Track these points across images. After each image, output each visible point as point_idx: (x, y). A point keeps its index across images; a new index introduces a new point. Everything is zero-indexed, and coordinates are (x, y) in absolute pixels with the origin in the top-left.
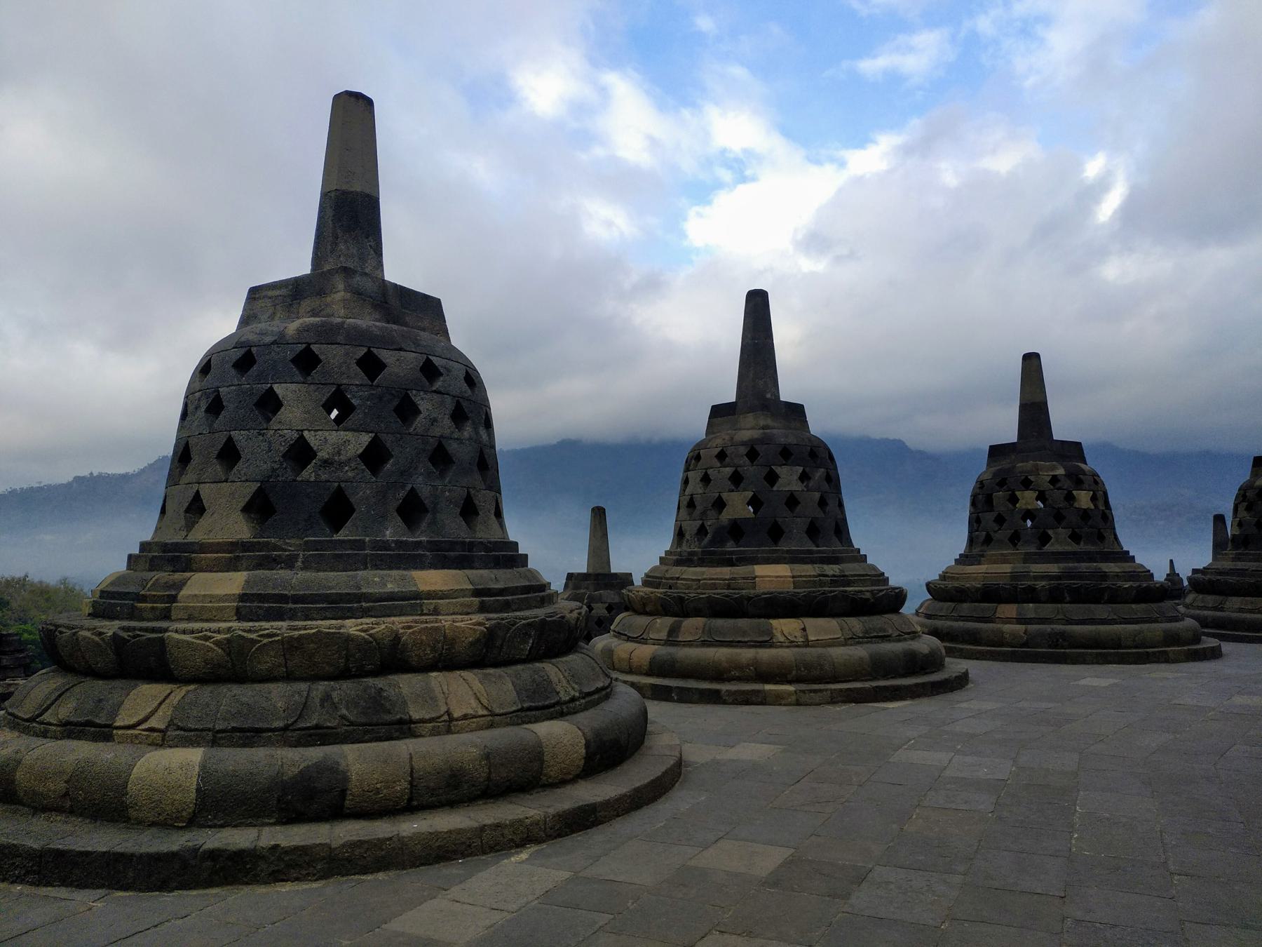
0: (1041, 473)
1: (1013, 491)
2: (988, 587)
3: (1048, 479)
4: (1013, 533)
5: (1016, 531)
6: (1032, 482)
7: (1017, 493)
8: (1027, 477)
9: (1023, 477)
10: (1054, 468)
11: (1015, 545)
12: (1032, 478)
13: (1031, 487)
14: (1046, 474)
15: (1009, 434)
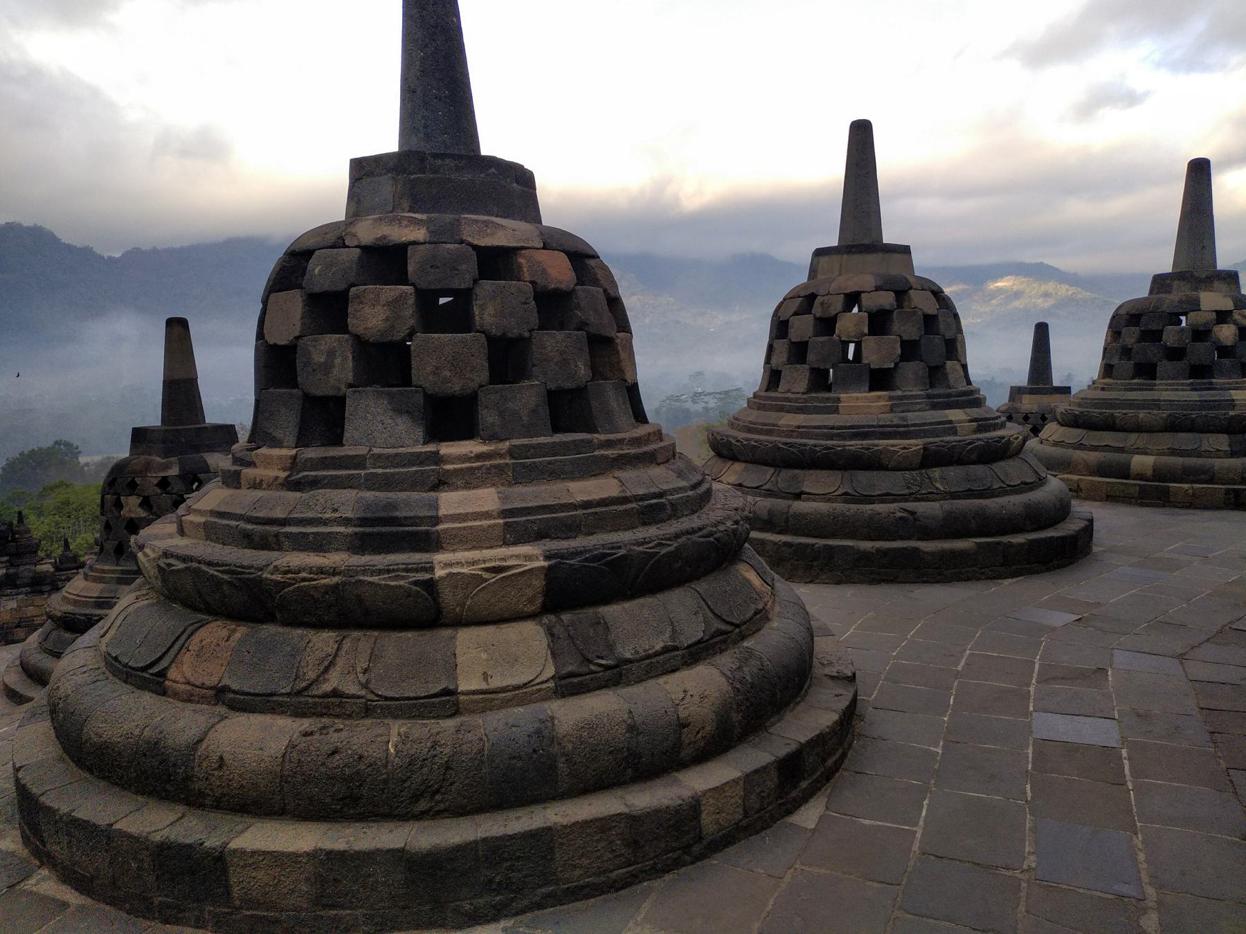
0: (148, 475)
1: (119, 495)
2: (66, 617)
3: (155, 482)
4: (118, 544)
5: (120, 542)
6: (138, 485)
7: (122, 498)
8: (134, 478)
9: (130, 479)
10: (167, 467)
11: (118, 559)
12: (138, 480)
13: (136, 492)
14: (154, 475)
15: (152, 417)
